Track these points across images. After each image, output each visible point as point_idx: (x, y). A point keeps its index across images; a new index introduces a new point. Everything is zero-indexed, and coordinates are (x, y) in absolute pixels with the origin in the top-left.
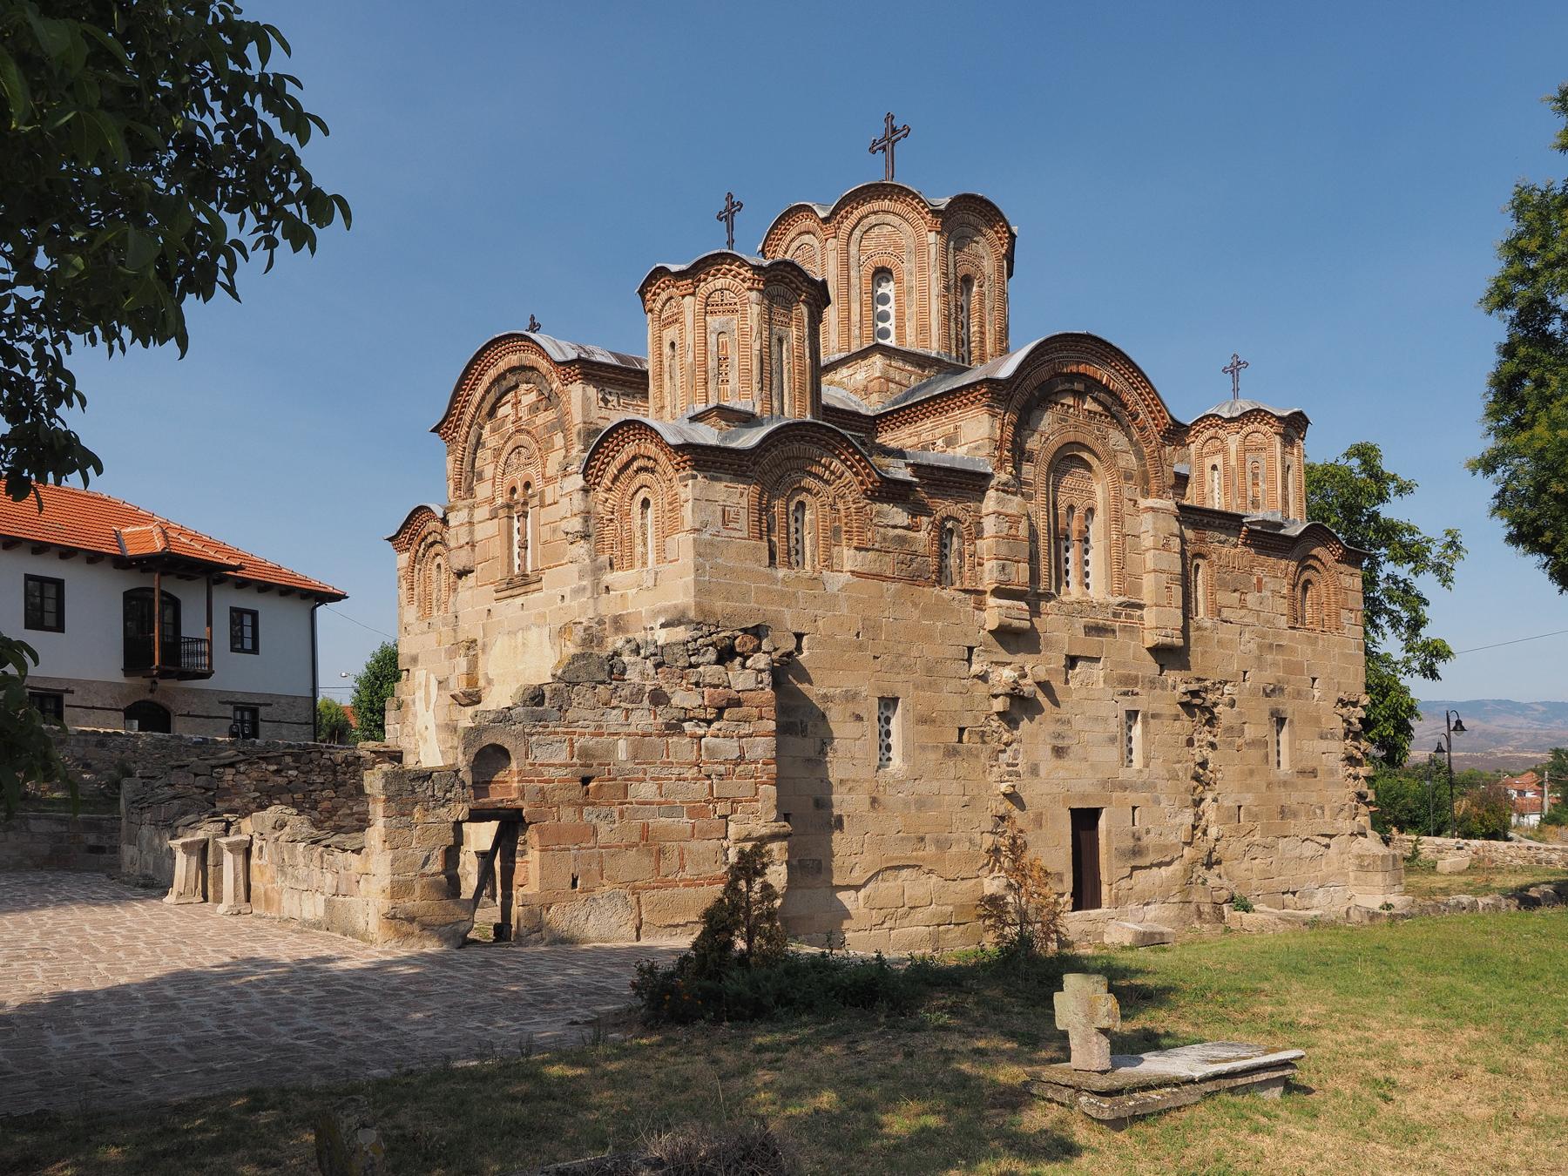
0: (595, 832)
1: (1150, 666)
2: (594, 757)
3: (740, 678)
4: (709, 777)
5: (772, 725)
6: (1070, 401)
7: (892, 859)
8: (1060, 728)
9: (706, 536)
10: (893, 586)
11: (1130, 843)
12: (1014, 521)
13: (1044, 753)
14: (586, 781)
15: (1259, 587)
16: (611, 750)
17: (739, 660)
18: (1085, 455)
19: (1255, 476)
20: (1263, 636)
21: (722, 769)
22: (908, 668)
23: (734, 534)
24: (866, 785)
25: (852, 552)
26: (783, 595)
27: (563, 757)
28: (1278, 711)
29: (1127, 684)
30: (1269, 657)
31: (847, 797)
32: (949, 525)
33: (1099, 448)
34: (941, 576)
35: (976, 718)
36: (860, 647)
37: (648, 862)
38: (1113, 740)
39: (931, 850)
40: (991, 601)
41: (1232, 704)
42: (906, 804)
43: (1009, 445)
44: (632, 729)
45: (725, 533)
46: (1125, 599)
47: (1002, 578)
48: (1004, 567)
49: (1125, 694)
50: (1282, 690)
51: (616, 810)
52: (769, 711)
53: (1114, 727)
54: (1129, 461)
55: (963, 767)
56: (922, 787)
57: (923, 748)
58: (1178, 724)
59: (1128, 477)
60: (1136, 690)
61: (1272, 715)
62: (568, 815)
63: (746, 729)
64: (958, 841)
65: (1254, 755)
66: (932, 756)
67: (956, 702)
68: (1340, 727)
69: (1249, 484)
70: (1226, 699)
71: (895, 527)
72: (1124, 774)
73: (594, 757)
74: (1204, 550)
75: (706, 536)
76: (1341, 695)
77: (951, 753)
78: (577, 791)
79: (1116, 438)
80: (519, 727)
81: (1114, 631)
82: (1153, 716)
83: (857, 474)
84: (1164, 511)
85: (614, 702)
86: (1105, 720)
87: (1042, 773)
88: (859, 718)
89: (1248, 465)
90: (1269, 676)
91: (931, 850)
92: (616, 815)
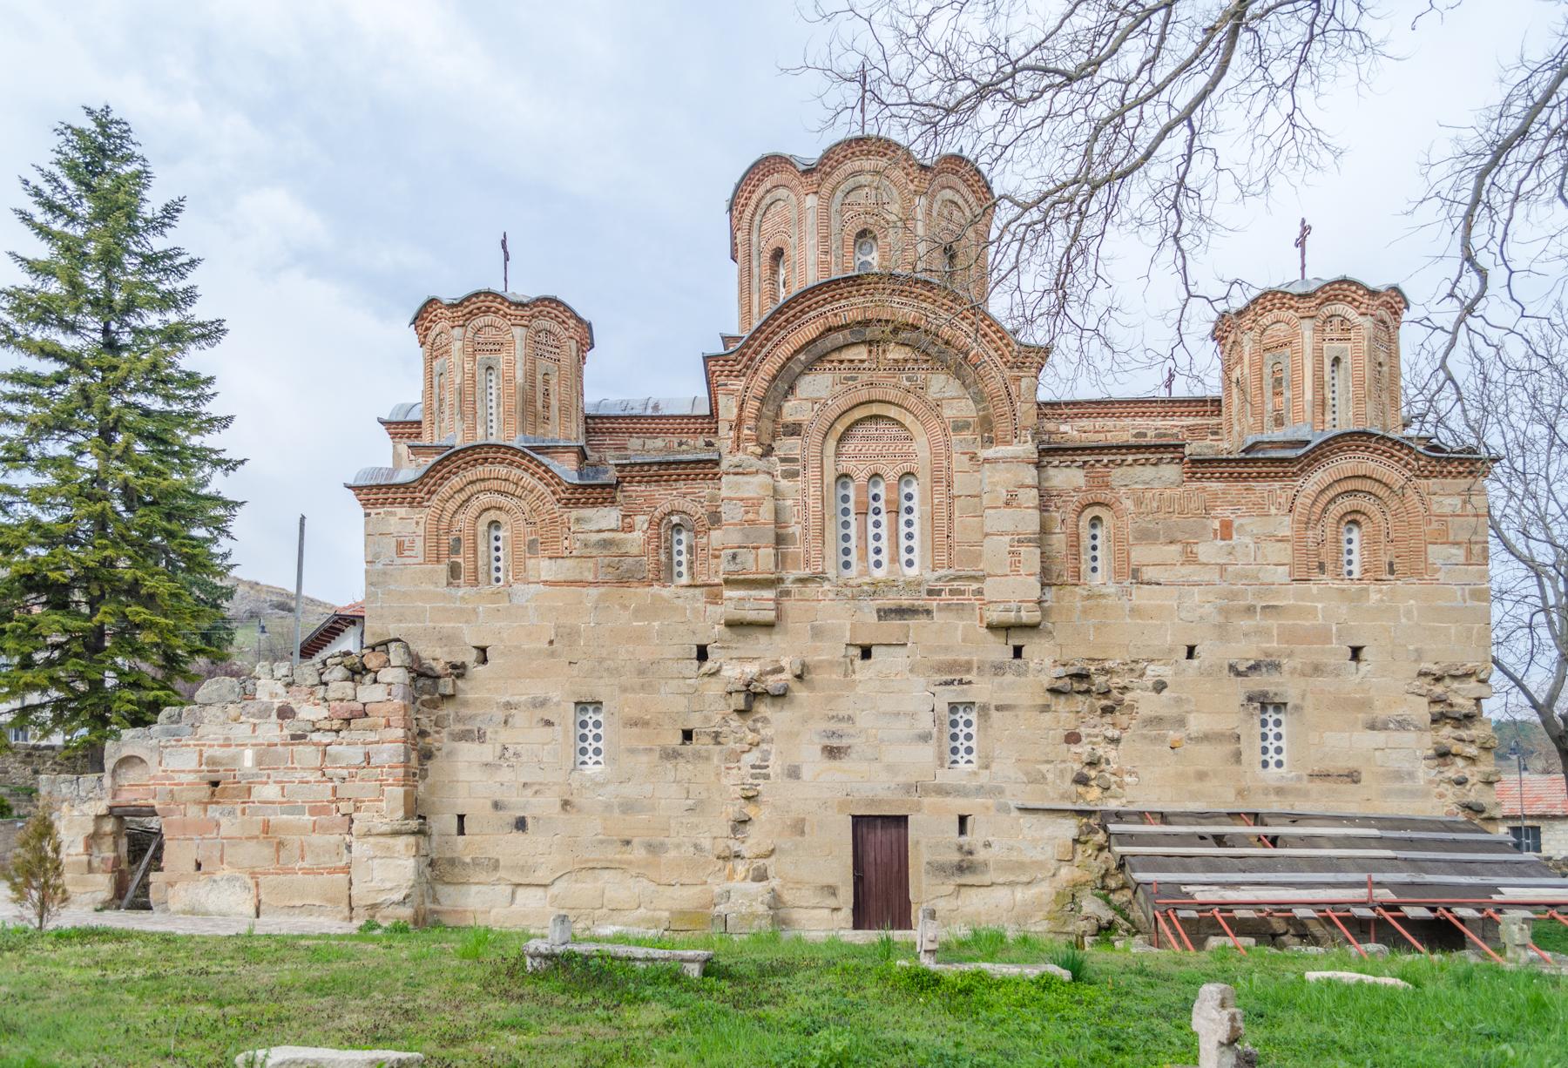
0: (218, 825)
1: (999, 650)
2: (221, 764)
3: (369, 693)
4: (331, 779)
5: (400, 733)
6: (860, 353)
7: (587, 861)
8: (833, 726)
9: (379, 566)
10: (593, 592)
11: (956, 857)
12: (753, 504)
13: (809, 755)
14: (215, 784)
15: (1226, 530)
16: (235, 759)
17: (370, 677)
18: (893, 412)
19: (1279, 382)
20: (1233, 596)
21: (345, 773)
22: (615, 672)
23: (408, 561)
24: (556, 788)
25: (547, 562)
26: (461, 611)
27: (194, 765)
28: (1265, 694)
29: (953, 673)
30: (1246, 623)
31: (534, 800)
32: (675, 519)
33: (911, 400)
34: (665, 573)
35: (707, 719)
36: (552, 654)
37: (268, 851)
38: (925, 738)
39: (638, 853)
40: (727, 593)
41: (1160, 686)
42: (608, 807)
43: (752, 423)
44: (260, 741)
45: (399, 561)
46: (952, 571)
47: (732, 568)
48: (734, 557)
49: (946, 683)
50: (1276, 666)
51: (239, 807)
52: (397, 719)
53: (926, 723)
54: (965, 408)
55: (685, 769)
56: (629, 791)
57: (632, 751)
58: (1047, 716)
59: (960, 426)
60: (966, 678)
61: (1250, 699)
62: (194, 812)
63: (372, 737)
64: (678, 846)
65: (1209, 756)
66: (644, 759)
67: (680, 704)
68: (1421, 711)
69: (1268, 392)
70: (1148, 681)
71: (600, 531)
72: (946, 777)
73: (221, 764)
74: (1102, 496)
75: (379, 566)
76: (1426, 666)
77: (670, 755)
78: (206, 790)
79: (940, 384)
80: (155, 741)
81: (928, 612)
82: (998, 708)
83: (547, 485)
84: (1015, 459)
85: (243, 718)
86: (913, 715)
87: (806, 773)
88: (549, 723)
89: (1267, 371)
90: (1245, 651)
91: (638, 853)
92: (239, 812)
